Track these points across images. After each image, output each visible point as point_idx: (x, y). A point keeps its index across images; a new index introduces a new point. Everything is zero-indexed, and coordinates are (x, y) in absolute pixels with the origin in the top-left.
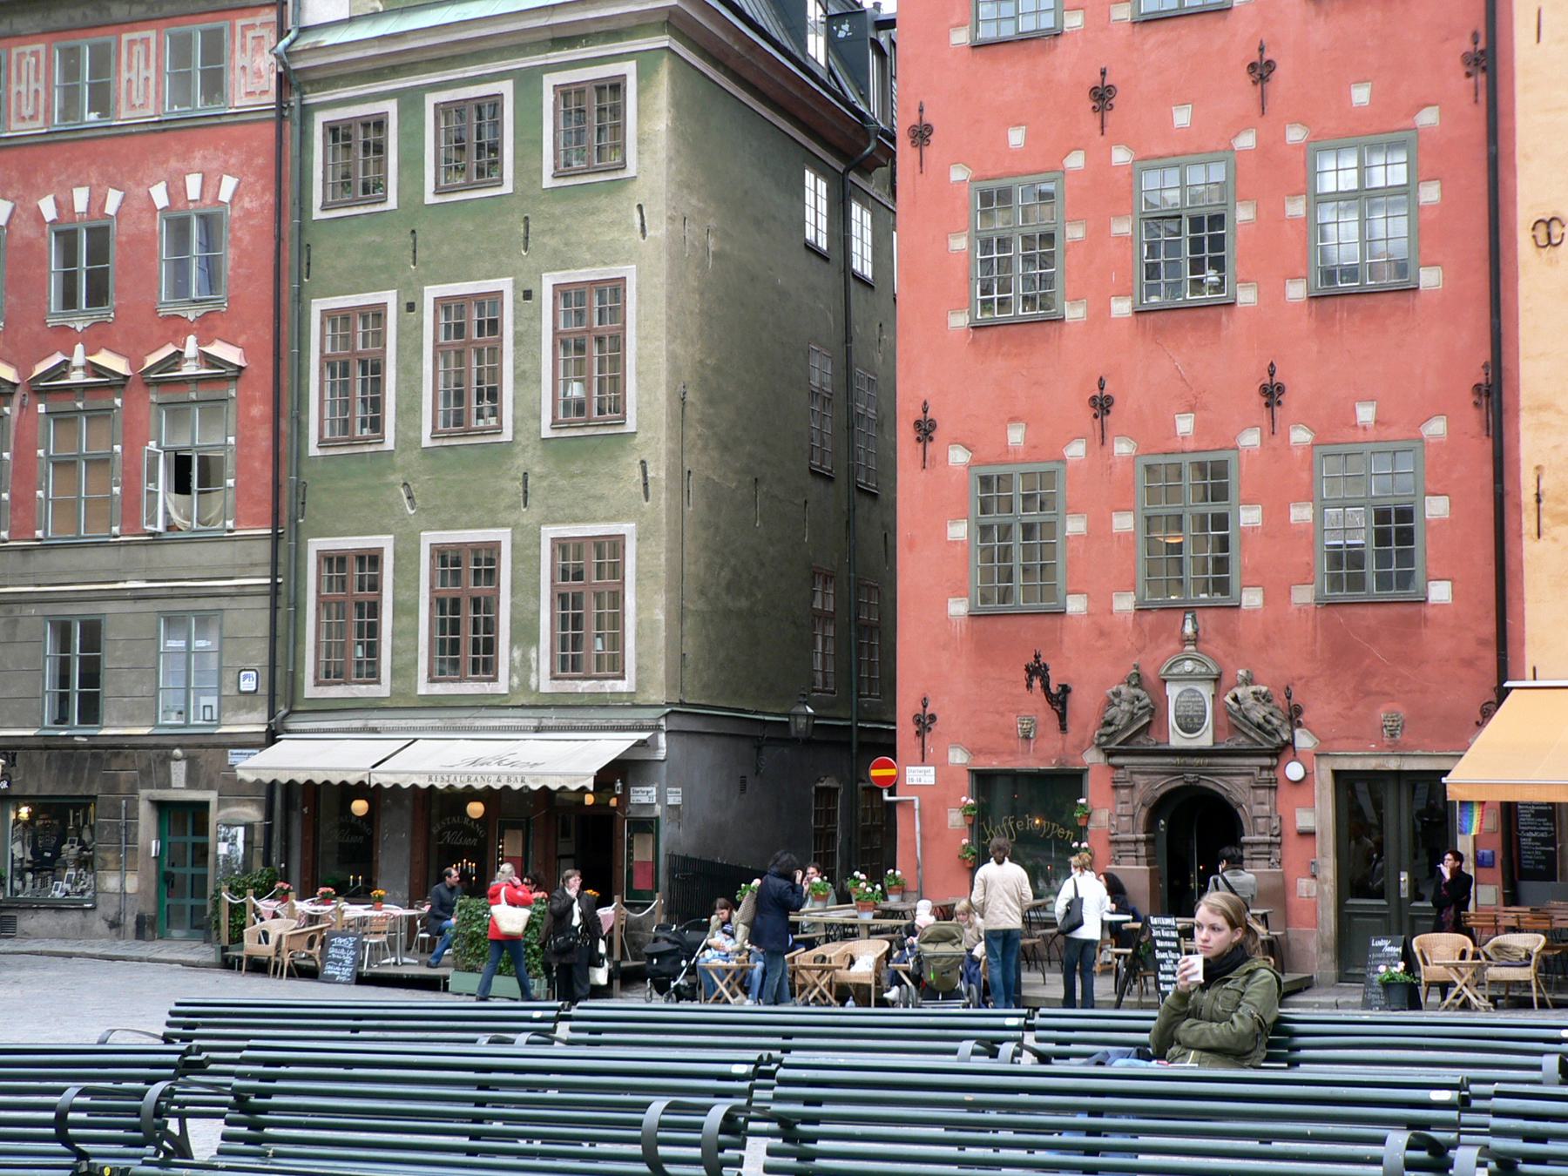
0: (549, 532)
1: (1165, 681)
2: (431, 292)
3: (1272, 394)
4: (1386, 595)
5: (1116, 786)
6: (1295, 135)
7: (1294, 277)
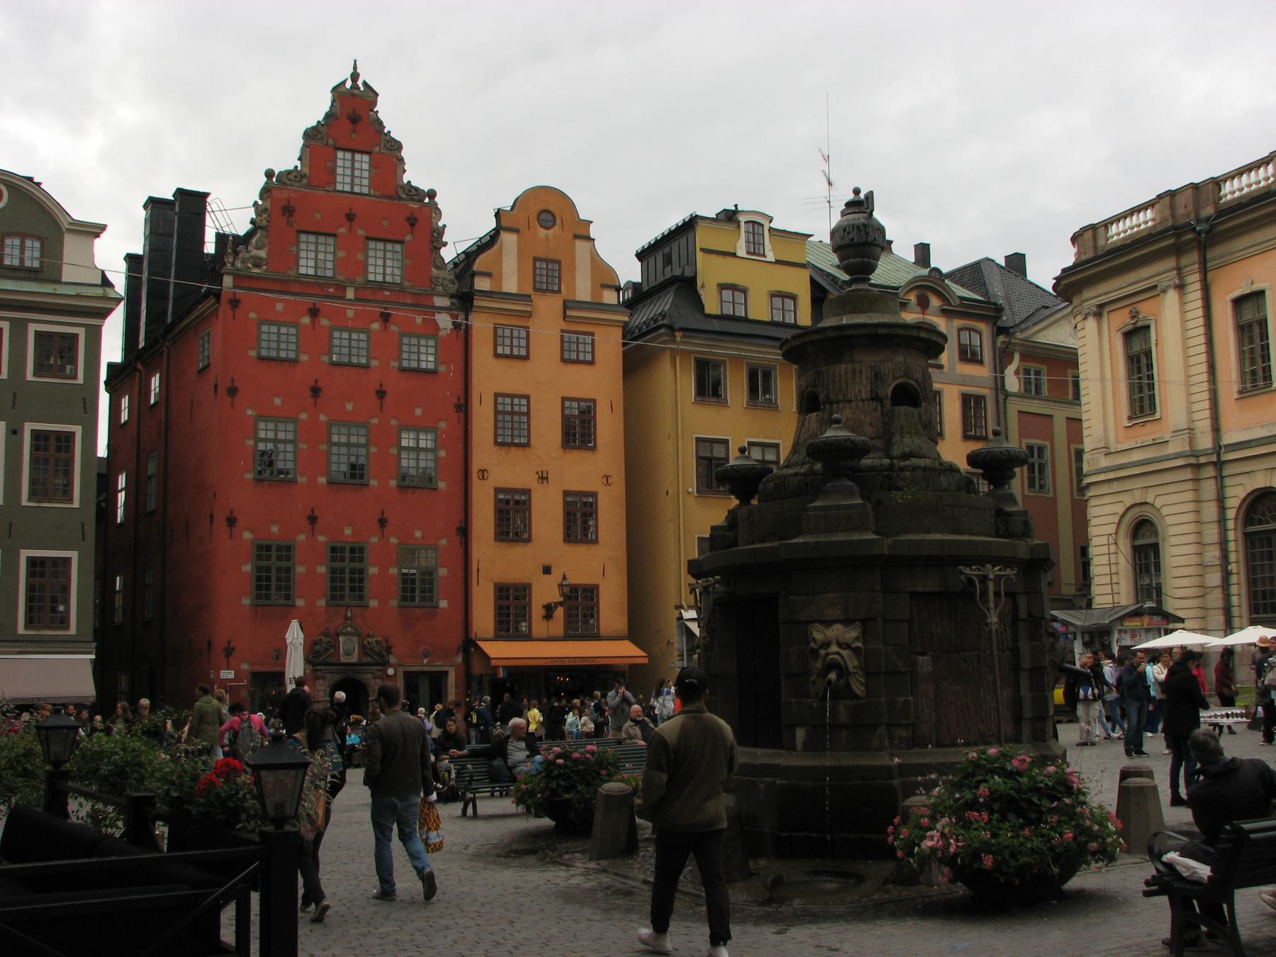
0: (25, 554)
1: (338, 635)
3: (383, 522)
4: (424, 604)
5: (317, 678)
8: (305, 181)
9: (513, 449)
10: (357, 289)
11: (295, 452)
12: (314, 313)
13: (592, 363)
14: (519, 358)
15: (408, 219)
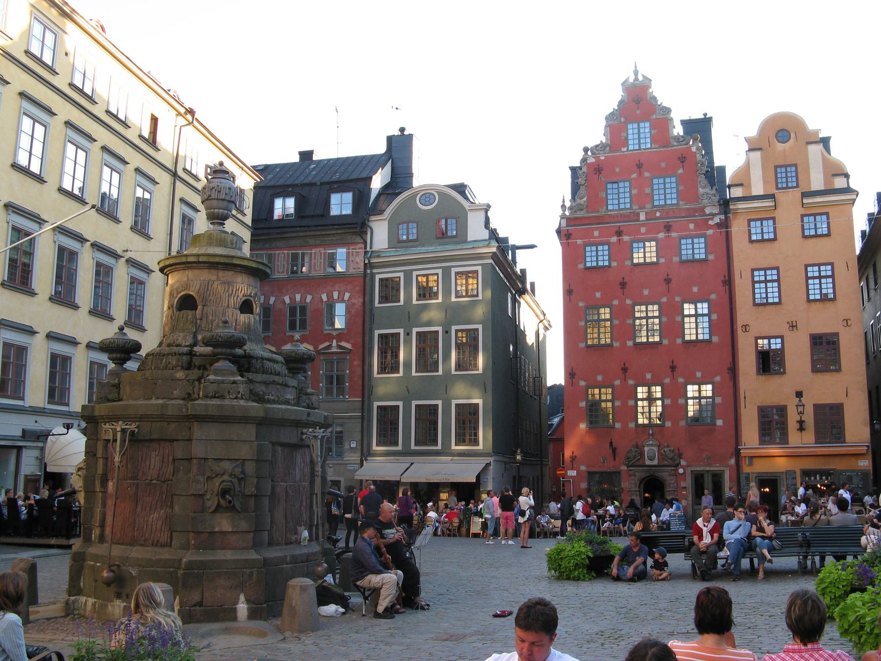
2: (415, 330)
3: (673, 368)
6: (677, 299)
7: (678, 337)
8: (608, 149)
9: (768, 307)
10: (647, 213)
11: (611, 326)
12: (619, 233)
13: (828, 235)
14: (769, 240)
15: (679, 158)
